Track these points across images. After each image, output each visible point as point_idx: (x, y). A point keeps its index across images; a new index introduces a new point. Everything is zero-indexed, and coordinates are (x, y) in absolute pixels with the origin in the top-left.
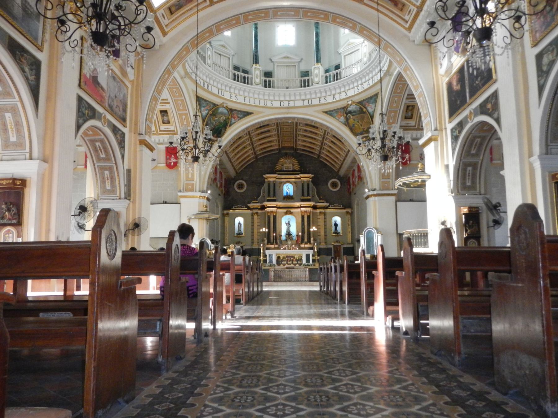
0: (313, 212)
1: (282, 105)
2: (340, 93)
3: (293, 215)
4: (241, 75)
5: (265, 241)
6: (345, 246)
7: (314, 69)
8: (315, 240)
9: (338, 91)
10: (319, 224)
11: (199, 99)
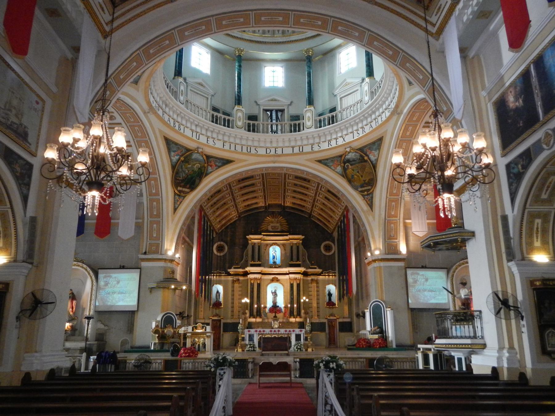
1: (268, 151)
2: (336, 139)
4: (221, 117)
5: (246, 313)
6: (341, 320)
7: (306, 111)
8: (306, 313)
9: (334, 136)
10: (310, 293)
11: (168, 142)
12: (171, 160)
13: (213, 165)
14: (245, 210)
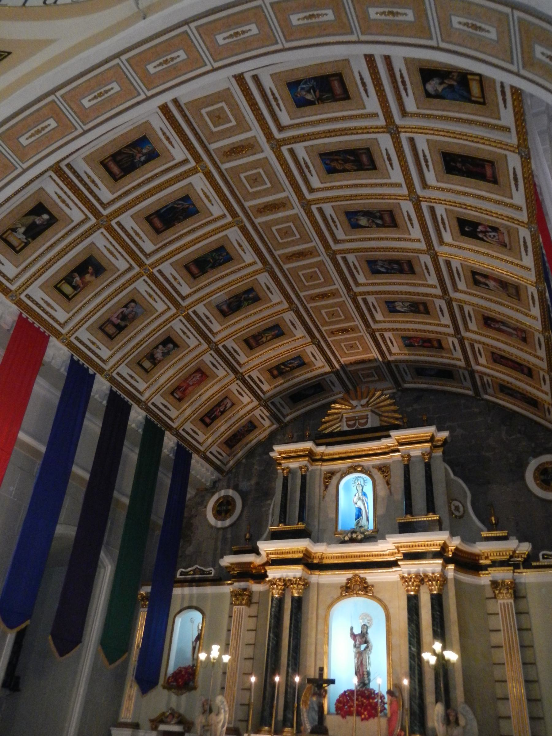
0: (457, 582)
3: (374, 598)
10: (497, 638)
14: (278, 389)
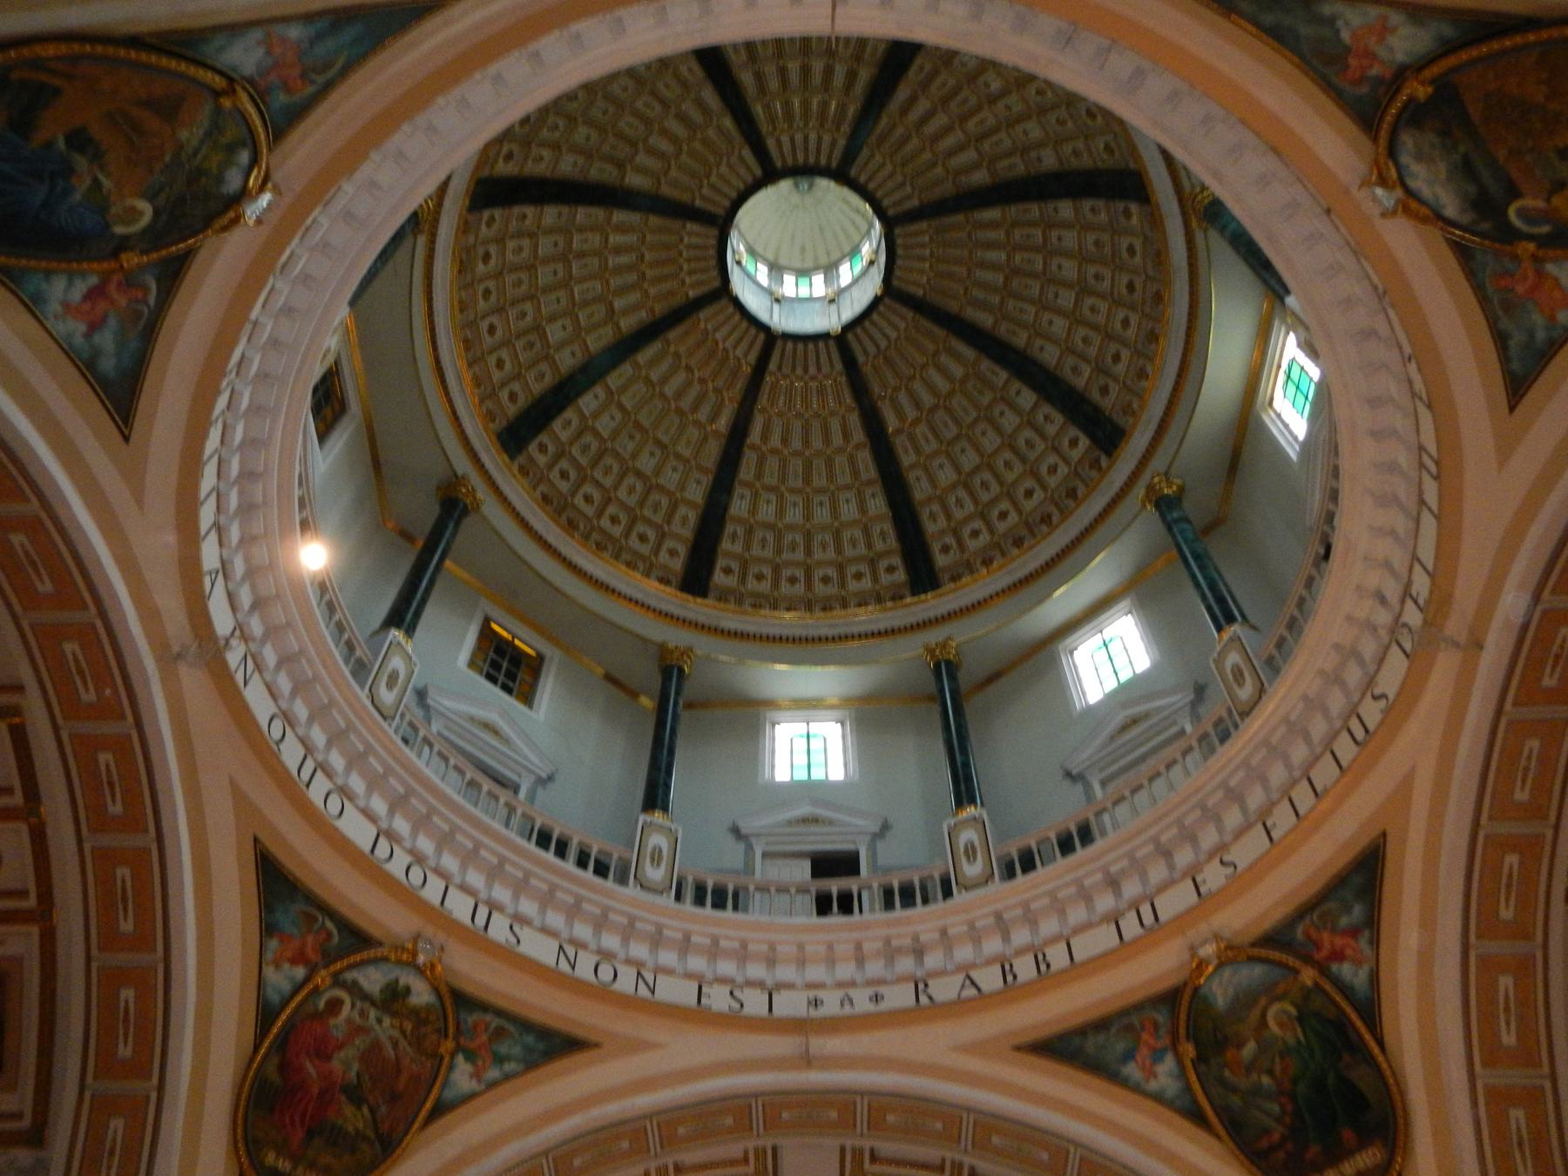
12: (1158, 1098)
13: (1339, 941)
